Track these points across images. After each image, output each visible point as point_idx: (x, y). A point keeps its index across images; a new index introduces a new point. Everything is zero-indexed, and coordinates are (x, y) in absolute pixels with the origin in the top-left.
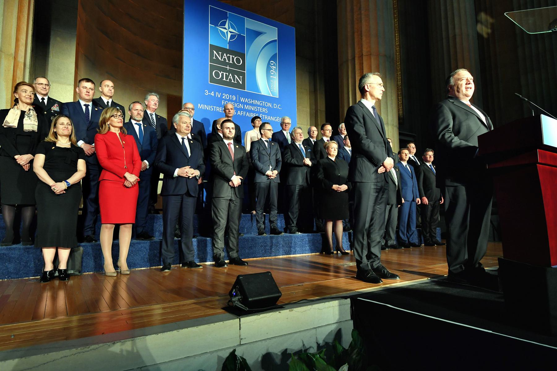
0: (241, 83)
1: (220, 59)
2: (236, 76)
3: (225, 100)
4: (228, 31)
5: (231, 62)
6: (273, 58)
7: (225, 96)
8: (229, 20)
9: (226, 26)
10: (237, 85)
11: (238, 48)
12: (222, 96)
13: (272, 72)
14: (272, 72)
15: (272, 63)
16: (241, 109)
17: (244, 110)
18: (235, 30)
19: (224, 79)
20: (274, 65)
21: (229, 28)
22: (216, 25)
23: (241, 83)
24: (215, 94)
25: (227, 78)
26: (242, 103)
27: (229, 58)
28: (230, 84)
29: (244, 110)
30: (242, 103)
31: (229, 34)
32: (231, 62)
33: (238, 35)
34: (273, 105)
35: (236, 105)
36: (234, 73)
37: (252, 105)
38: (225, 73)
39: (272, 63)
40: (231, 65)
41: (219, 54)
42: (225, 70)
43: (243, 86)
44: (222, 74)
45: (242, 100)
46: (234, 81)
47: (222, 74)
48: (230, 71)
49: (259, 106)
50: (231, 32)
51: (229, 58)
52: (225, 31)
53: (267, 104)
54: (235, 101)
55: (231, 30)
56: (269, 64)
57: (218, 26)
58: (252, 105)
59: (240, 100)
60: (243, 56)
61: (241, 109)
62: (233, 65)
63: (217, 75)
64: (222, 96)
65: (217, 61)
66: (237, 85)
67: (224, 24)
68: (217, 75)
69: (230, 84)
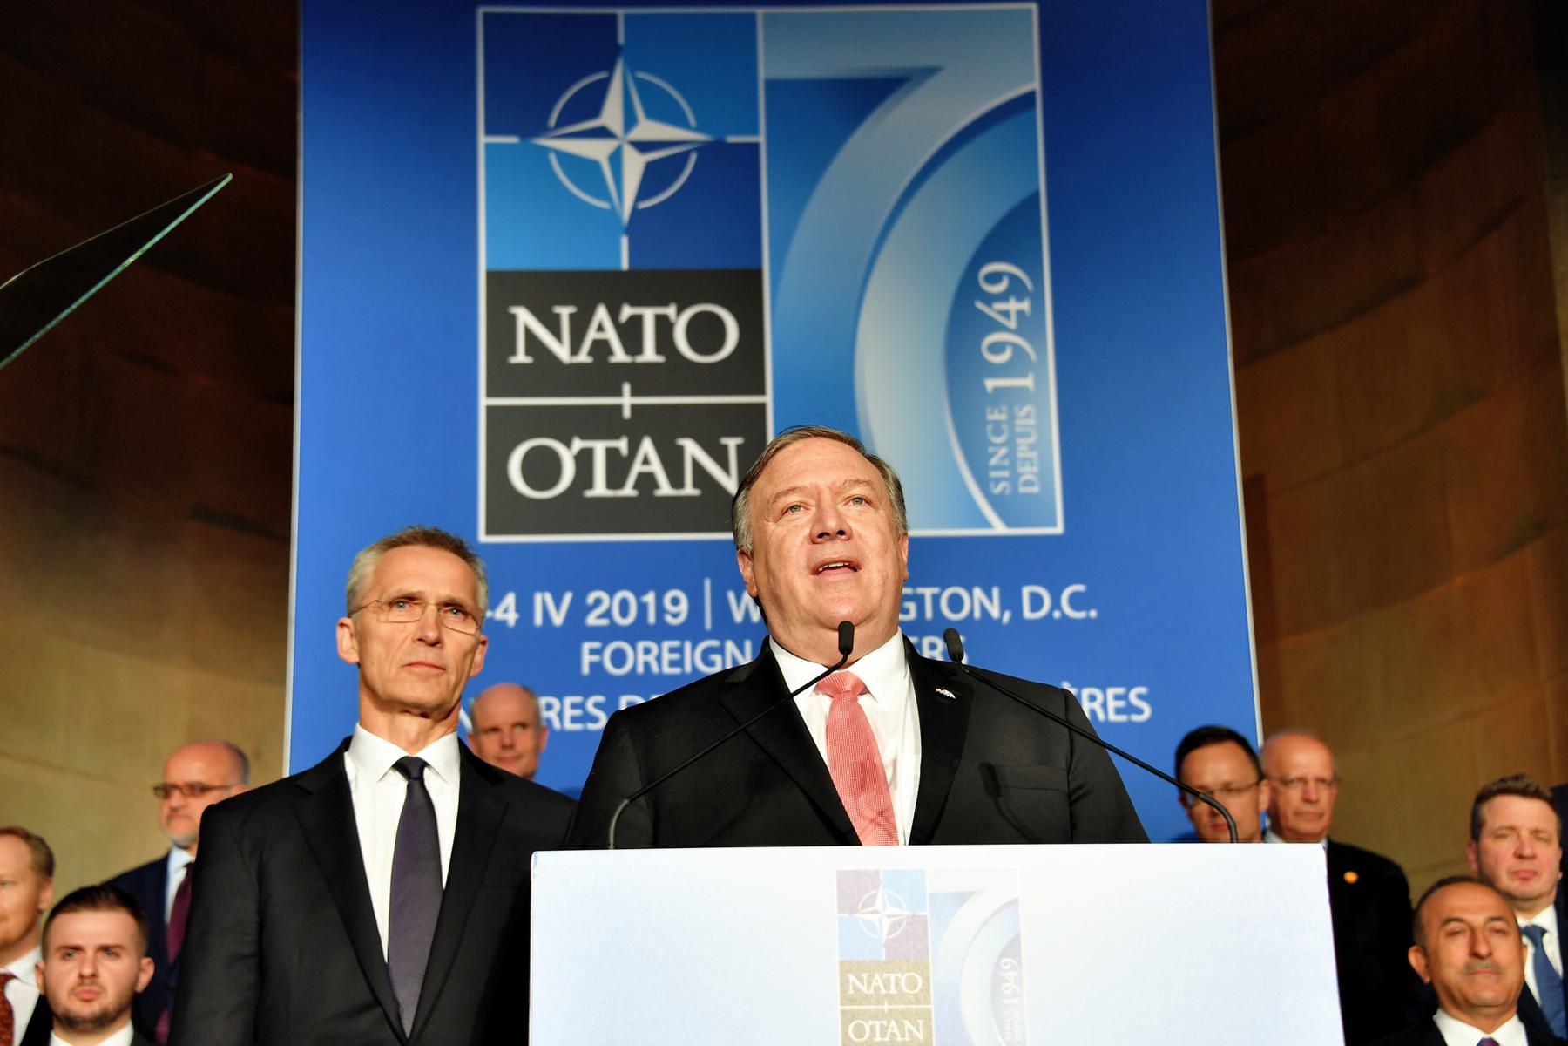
1: (562, 351)
2: (691, 448)
3: (608, 634)
4: (621, 146)
5: (650, 354)
6: (1008, 237)
7: (606, 605)
8: (632, 67)
9: (612, 114)
11: (704, 247)
12: (579, 610)
13: (997, 348)
14: (997, 348)
15: (994, 278)
18: (679, 120)
19: (600, 489)
20: (1016, 289)
21: (630, 121)
22: (532, 125)
24: (524, 607)
25: (615, 480)
27: (631, 334)
31: (634, 165)
32: (650, 354)
33: (703, 150)
34: (1011, 601)
36: (664, 428)
38: (600, 448)
39: (994, 278)
40: (645, 380)
41: (553, 325)
42: (604, 423)
44: (584, 459)
46: (676, 480)
47: (584, 459)
48: (643, 423)
50: (643, 147)
51: (631, 334)
52: (597, 150)
53: (956, 603)
54: (691, 631)
55: (649, 129)
56: (968, 290)
57: (542, 129)
59: (722, 609)
60: (744, 293)
62: (673, 374)
63: (542, 468)
64: (579, 610)
65: (545, 372)
67: (591, 103)
68: (542, 468)
69: (647, 510)
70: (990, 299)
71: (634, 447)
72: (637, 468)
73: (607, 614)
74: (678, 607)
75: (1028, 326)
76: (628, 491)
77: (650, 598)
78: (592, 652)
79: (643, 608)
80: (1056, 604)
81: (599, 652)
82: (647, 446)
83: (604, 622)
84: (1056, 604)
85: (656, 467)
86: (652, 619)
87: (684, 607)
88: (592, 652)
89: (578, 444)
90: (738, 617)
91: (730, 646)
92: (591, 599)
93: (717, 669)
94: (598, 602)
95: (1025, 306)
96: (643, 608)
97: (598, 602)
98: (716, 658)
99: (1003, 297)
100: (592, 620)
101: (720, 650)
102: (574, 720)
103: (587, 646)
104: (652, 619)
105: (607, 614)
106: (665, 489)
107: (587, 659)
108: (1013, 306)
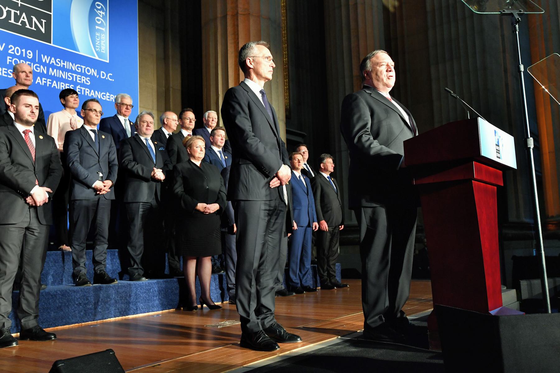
0: (43, 30)
2: (34, 19)
3: (14, 56)
7: (13, 50)
10: (37, 34)
12: (6, 49)
13: (98, 20)
14: (98, 20)
15: (98, 5)
16: (42, 75)
17: (47, 76)
19: (12, 21)
20: (102, 9)
23: (43, 30)
25: (17, 19)
26: (45, 64)
28: (22, 29)
29: (47, 76)
30: (45, 64)
34: (99, 73)
35: (33, 67)
37: (63, 69)
38: (13, 11)
39: (98, 5)
43: (46, 37)
44: (9, 13)
45: (45, 59)
46: (31, 25)
47: (9, 13)
49: (75, 72)
53: (88, 71)
54: (33, 60)
56: (93, 7)
58: (63, 69)
61: (42, 75)
64: (6, 49)
66: (37, 34)
69: (22, 29)
70: (98, 9)
71: (21, 14)
72: (22, 19)
73: (14, 51)
74: (30, 56)
75: (104, 17)
76: (19, 24)
77: (24, 50)
78: (10, 59)
79: (22, 52)
80: (107, 77)
81: (12, 60)
82: (24, 15)
83: (13, 53)
84: (107, 77)
85: (26, 20)
86: (24, 56)
87: (31, 55)
88: (10, 59)
89: (7, 9)
90: (44, 61)
91: (42, 67)
92: (9, 47)
93: (39, 71)
94: (11, 48)
95: (104, 13)
96: (22, 52)
97: (11, 48)
98: (39, 69)
99: (100, 10)
100: (10, 52)
101: (40, 67)
102: (5, 74)
103: (8, 57)
104: (24, 56)
105: (14, 51)
106: (28, 26)
107: (8, 60)
108: (101, 12)
